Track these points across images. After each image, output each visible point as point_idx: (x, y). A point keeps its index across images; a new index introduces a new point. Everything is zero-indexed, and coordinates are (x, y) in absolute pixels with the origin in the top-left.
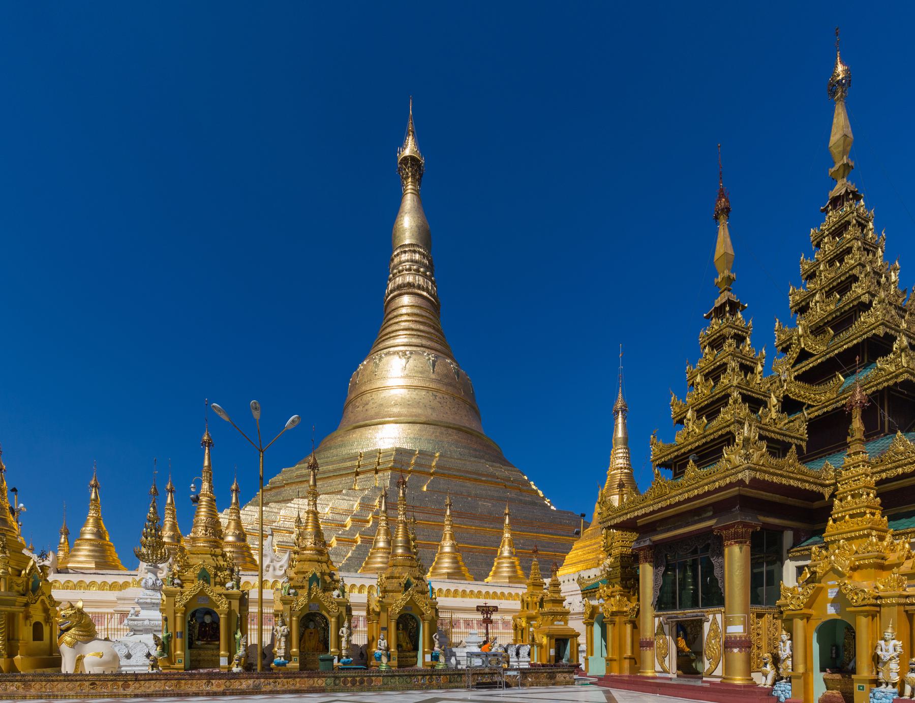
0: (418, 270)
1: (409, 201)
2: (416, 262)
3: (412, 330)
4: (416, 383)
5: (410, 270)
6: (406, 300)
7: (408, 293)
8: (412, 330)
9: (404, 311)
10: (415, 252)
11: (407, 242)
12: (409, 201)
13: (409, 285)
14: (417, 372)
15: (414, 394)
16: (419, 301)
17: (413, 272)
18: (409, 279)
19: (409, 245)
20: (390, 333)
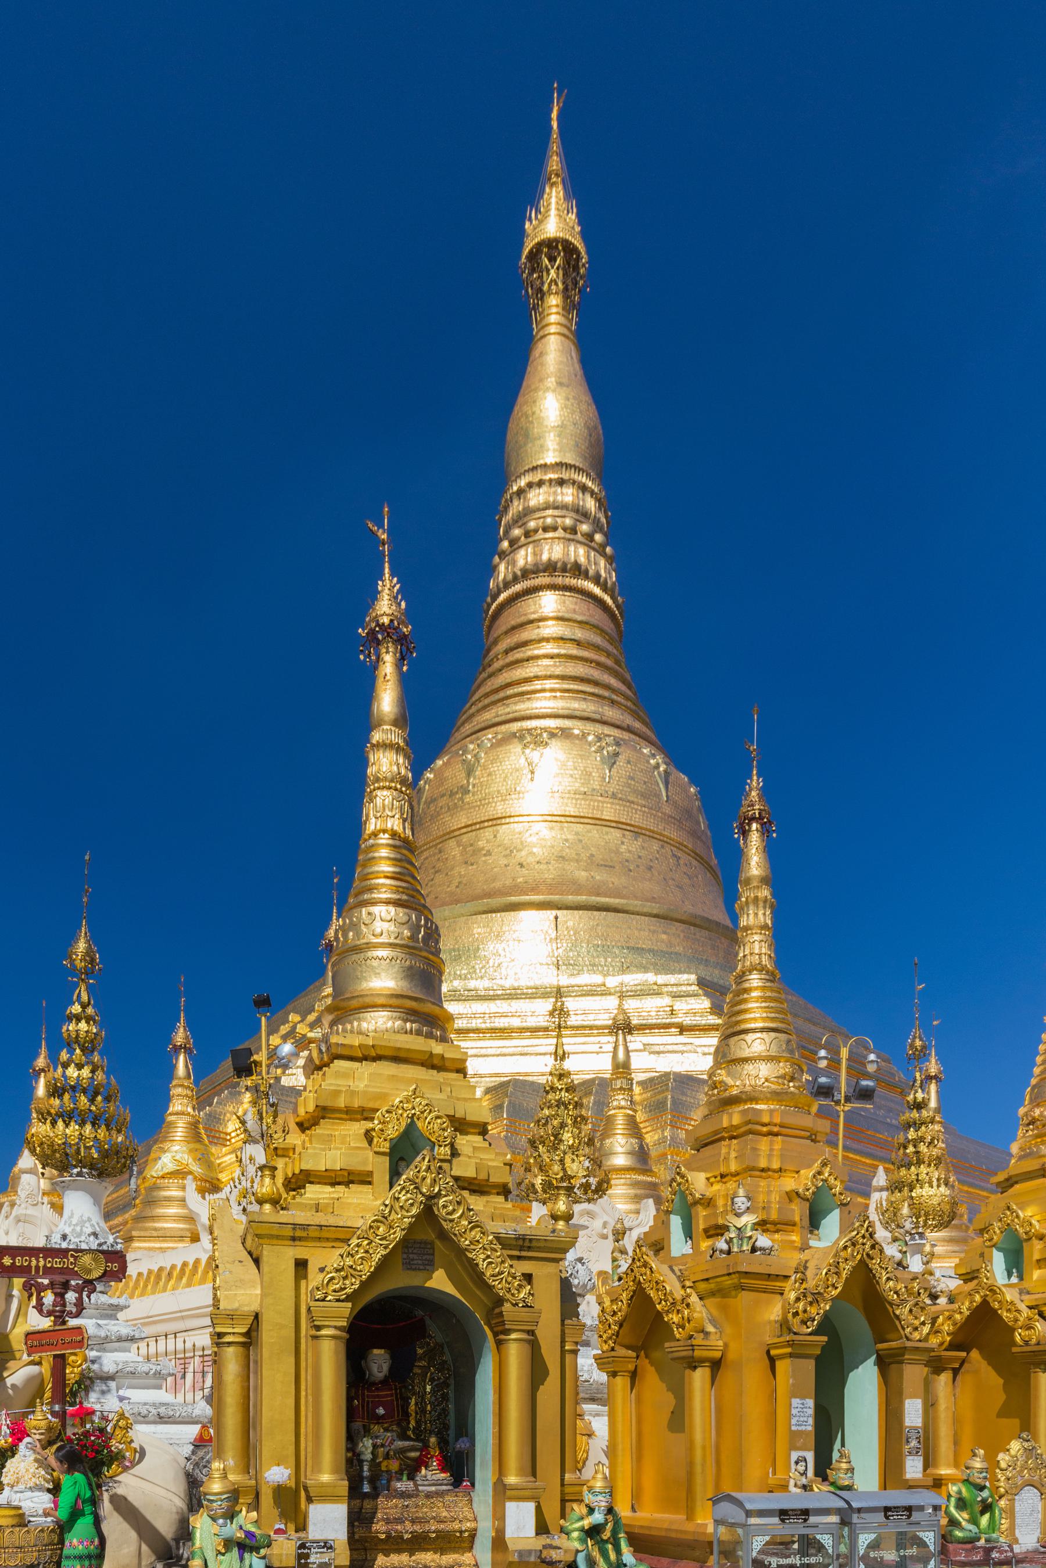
0: (590, 537)
1: (554, 352)
2: (583, 514)
3: (596, 683)
4: (637, 819)
5: (573, 530)
6: (549, 603)
7: (553, 587)
8: (596, 683)
9: (551, 629)
10: (561, 482)
11: (550, 458)
12: (554, 352)
13: (551, 567)
14: (635, 791)
15: (630, 847)
16: (597, 616)
17: (560, 533)
18: (553, 550)
19: (560, 465)
20: (527, 680)
